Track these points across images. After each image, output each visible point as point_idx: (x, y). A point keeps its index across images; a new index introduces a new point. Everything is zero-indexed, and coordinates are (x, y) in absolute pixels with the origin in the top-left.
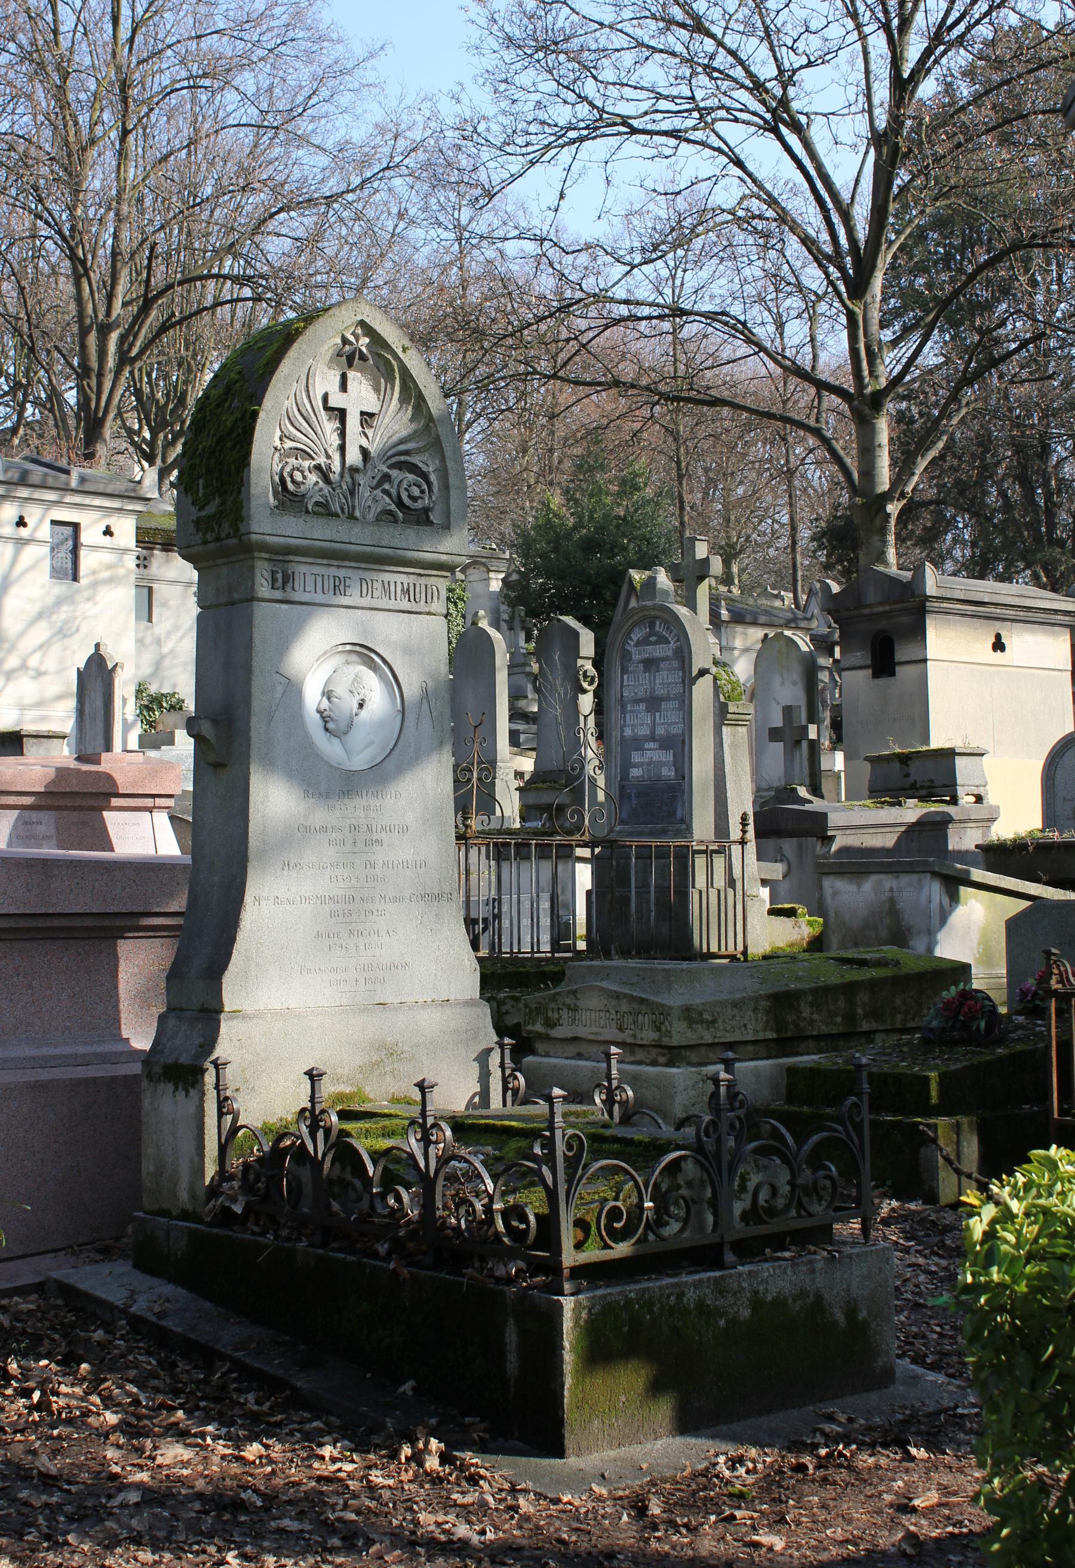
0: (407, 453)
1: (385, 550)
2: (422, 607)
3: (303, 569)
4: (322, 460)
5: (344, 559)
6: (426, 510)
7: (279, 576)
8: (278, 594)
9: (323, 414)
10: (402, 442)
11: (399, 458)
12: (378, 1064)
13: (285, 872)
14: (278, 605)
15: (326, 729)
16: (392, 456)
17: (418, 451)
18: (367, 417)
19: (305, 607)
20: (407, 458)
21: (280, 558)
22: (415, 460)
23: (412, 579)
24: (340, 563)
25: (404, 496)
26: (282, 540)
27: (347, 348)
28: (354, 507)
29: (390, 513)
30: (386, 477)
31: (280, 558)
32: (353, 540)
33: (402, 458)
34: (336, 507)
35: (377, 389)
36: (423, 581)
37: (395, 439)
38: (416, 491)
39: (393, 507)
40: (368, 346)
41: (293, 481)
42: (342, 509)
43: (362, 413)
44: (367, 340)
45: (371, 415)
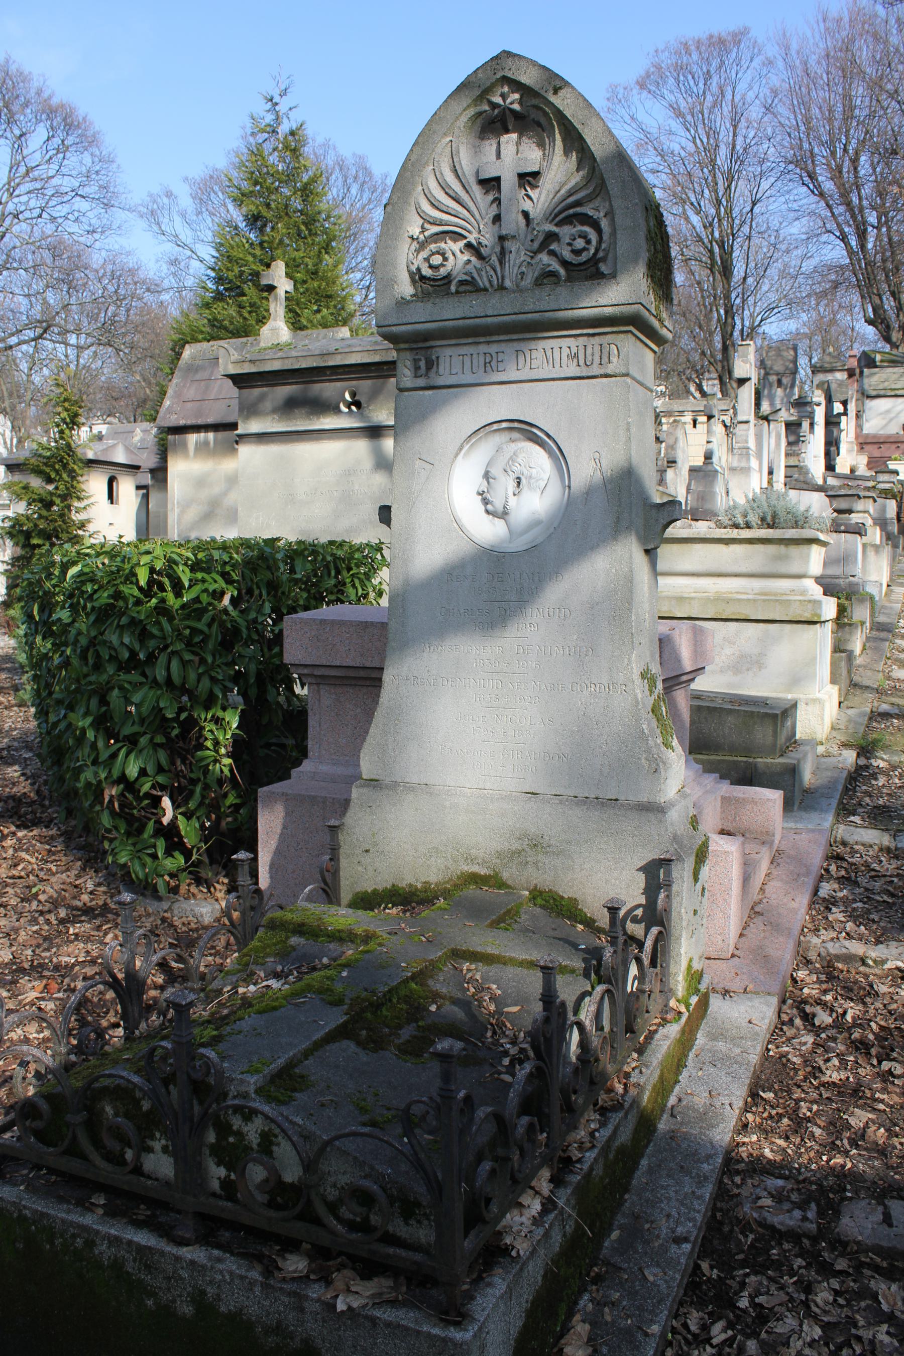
0: (578, 204)
1: (530, 316)
2: (596, 370)
3: (448, 352)
4: (472, 238)
5: (491, 334)
6: (594, 261)
7: (422, 364)
8: (421, 382)
9: (477, 190)
10: (570, 194)
11: (568, 213)
12: (519, 852)
13: (425, 654)
14: (421, 393)
15: (487, 512)
16: (560, 212)
17: (589, 198)
18: (528, 179)
19: (452, 390)
20: (578, 210)
21: (420, 345)
22: (588, 210)
23: (582, 341)
24: (488, 339)
25: (567, 254)
26: (409, 327)
27: (496, 111)
28: (503, 277)
29: (553, 274)
30: (551, 237)
31: (420, 345)
32: (490, 313)
33: (571, 211)
34: (483, 282)
35: (541, 145)
36: (596, 340)
37: (563, 192)
38: (580, 243)
39: (556, 266)
40: (521, 103)
41: (431, 267)
42: (490, 282)
43: (522, 176)
44: (517, 96)
45: (536, 175)
